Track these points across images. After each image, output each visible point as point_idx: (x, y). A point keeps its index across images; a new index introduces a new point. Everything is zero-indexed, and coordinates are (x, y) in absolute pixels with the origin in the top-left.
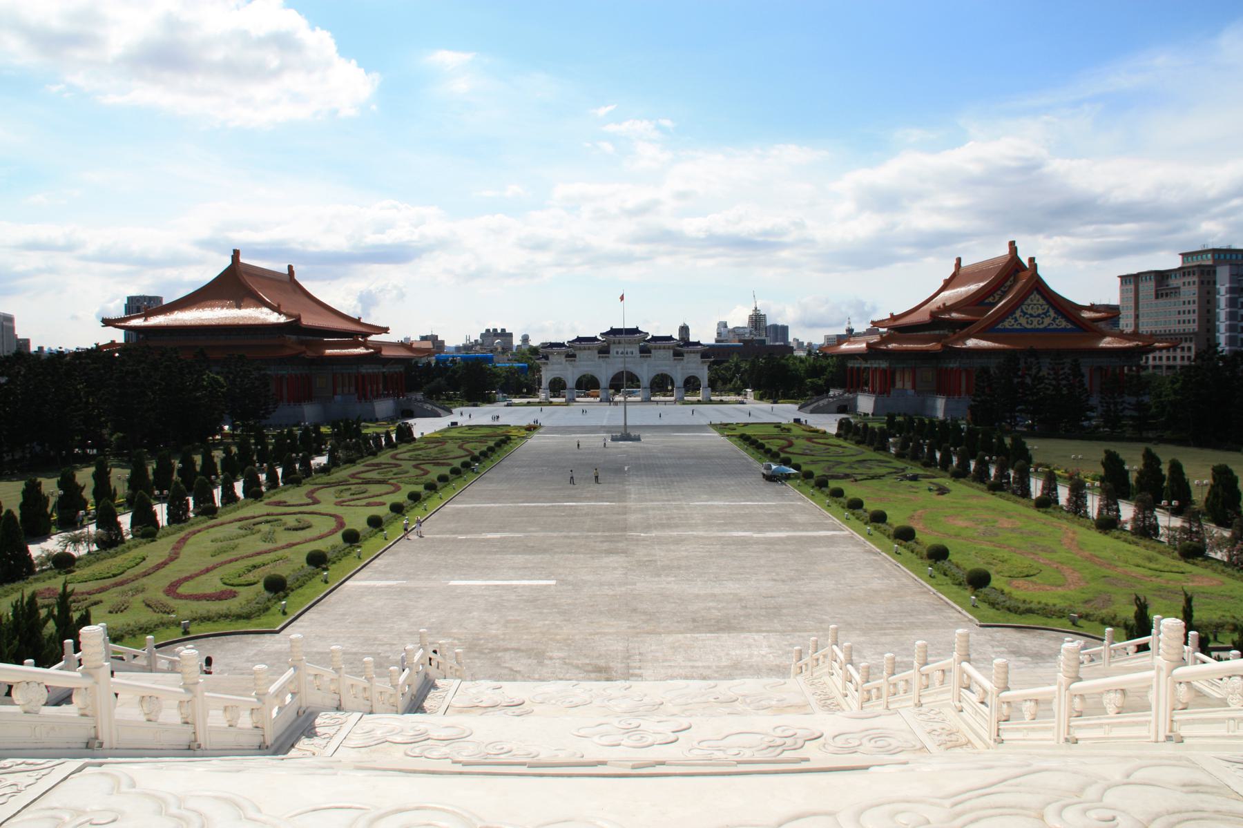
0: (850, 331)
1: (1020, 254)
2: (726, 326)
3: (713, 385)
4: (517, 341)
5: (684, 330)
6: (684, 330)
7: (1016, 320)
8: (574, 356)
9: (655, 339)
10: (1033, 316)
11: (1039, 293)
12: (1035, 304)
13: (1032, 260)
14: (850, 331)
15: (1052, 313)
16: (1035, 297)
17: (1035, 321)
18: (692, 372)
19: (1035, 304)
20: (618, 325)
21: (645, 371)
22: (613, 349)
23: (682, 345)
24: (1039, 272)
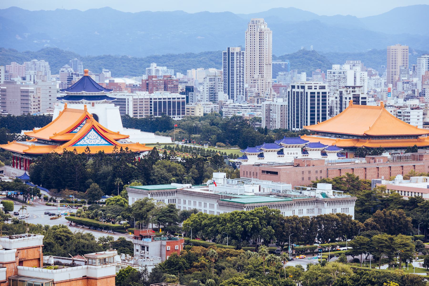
11: (95, 130)
15: (99, 137)
16: (93, 132)
17: (93, 141)
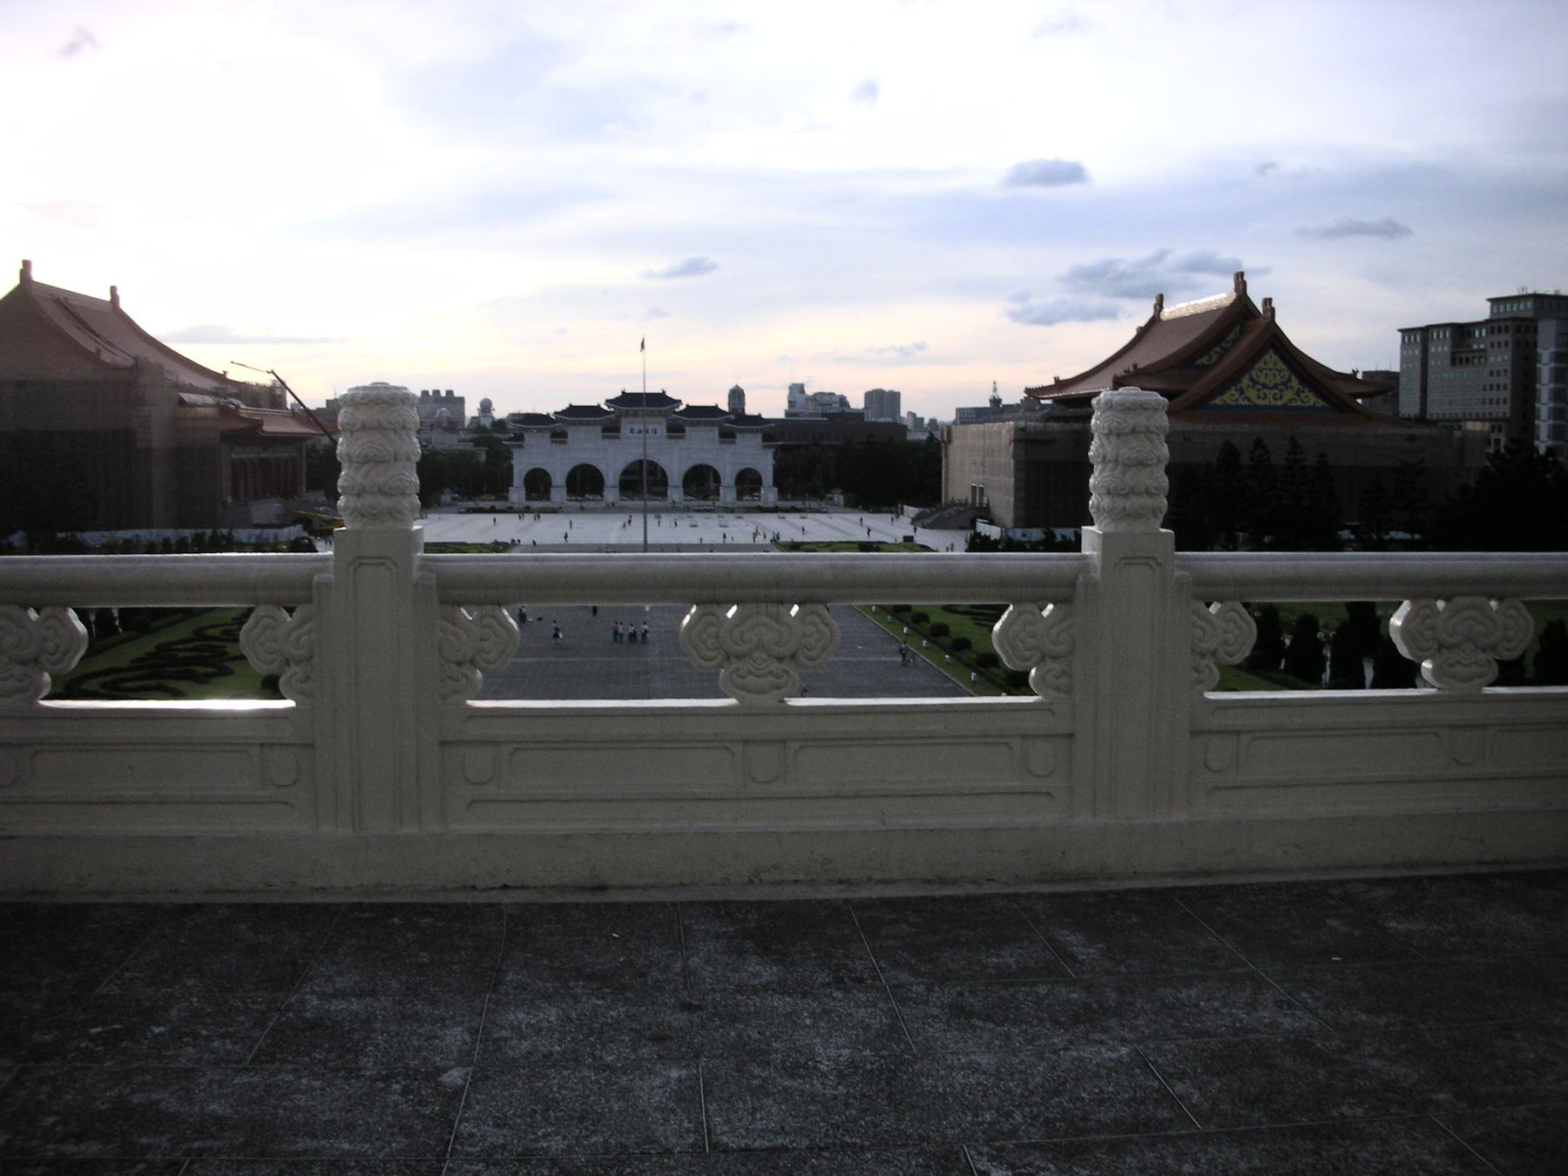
0: (996, 401)
1: (1250, 293)
2: (803, 391)
3: (778, 482)
4: (471, 410)
5: (737, 395)
6: (737, 395)
7: (1242, 392)
8: (564, 435)
9: (691, 410)
10: (1266, 387)
11: (1277, 352)
12: (1271, 367)
13: (1268, 302)
14: (996, 401)
15: (1295, 382)
16: (1271, 358)
18: (747, 462)
19: (1271, 367)
20: (635, 387)
21: (675, 461)
22: (626, 426)
23: (731, 420)
24: (1279, 321)
